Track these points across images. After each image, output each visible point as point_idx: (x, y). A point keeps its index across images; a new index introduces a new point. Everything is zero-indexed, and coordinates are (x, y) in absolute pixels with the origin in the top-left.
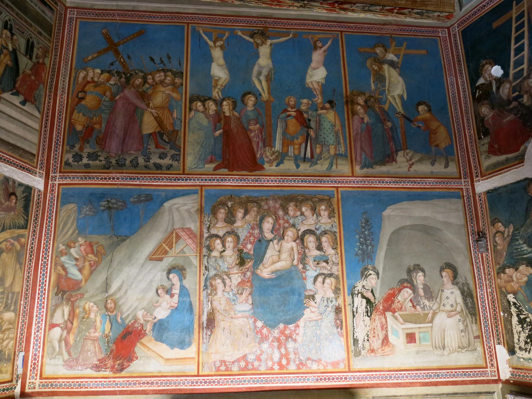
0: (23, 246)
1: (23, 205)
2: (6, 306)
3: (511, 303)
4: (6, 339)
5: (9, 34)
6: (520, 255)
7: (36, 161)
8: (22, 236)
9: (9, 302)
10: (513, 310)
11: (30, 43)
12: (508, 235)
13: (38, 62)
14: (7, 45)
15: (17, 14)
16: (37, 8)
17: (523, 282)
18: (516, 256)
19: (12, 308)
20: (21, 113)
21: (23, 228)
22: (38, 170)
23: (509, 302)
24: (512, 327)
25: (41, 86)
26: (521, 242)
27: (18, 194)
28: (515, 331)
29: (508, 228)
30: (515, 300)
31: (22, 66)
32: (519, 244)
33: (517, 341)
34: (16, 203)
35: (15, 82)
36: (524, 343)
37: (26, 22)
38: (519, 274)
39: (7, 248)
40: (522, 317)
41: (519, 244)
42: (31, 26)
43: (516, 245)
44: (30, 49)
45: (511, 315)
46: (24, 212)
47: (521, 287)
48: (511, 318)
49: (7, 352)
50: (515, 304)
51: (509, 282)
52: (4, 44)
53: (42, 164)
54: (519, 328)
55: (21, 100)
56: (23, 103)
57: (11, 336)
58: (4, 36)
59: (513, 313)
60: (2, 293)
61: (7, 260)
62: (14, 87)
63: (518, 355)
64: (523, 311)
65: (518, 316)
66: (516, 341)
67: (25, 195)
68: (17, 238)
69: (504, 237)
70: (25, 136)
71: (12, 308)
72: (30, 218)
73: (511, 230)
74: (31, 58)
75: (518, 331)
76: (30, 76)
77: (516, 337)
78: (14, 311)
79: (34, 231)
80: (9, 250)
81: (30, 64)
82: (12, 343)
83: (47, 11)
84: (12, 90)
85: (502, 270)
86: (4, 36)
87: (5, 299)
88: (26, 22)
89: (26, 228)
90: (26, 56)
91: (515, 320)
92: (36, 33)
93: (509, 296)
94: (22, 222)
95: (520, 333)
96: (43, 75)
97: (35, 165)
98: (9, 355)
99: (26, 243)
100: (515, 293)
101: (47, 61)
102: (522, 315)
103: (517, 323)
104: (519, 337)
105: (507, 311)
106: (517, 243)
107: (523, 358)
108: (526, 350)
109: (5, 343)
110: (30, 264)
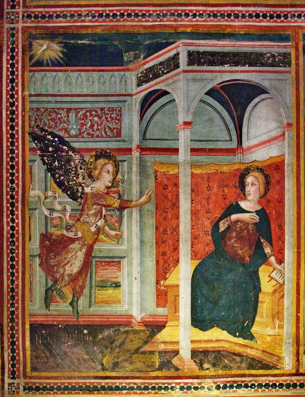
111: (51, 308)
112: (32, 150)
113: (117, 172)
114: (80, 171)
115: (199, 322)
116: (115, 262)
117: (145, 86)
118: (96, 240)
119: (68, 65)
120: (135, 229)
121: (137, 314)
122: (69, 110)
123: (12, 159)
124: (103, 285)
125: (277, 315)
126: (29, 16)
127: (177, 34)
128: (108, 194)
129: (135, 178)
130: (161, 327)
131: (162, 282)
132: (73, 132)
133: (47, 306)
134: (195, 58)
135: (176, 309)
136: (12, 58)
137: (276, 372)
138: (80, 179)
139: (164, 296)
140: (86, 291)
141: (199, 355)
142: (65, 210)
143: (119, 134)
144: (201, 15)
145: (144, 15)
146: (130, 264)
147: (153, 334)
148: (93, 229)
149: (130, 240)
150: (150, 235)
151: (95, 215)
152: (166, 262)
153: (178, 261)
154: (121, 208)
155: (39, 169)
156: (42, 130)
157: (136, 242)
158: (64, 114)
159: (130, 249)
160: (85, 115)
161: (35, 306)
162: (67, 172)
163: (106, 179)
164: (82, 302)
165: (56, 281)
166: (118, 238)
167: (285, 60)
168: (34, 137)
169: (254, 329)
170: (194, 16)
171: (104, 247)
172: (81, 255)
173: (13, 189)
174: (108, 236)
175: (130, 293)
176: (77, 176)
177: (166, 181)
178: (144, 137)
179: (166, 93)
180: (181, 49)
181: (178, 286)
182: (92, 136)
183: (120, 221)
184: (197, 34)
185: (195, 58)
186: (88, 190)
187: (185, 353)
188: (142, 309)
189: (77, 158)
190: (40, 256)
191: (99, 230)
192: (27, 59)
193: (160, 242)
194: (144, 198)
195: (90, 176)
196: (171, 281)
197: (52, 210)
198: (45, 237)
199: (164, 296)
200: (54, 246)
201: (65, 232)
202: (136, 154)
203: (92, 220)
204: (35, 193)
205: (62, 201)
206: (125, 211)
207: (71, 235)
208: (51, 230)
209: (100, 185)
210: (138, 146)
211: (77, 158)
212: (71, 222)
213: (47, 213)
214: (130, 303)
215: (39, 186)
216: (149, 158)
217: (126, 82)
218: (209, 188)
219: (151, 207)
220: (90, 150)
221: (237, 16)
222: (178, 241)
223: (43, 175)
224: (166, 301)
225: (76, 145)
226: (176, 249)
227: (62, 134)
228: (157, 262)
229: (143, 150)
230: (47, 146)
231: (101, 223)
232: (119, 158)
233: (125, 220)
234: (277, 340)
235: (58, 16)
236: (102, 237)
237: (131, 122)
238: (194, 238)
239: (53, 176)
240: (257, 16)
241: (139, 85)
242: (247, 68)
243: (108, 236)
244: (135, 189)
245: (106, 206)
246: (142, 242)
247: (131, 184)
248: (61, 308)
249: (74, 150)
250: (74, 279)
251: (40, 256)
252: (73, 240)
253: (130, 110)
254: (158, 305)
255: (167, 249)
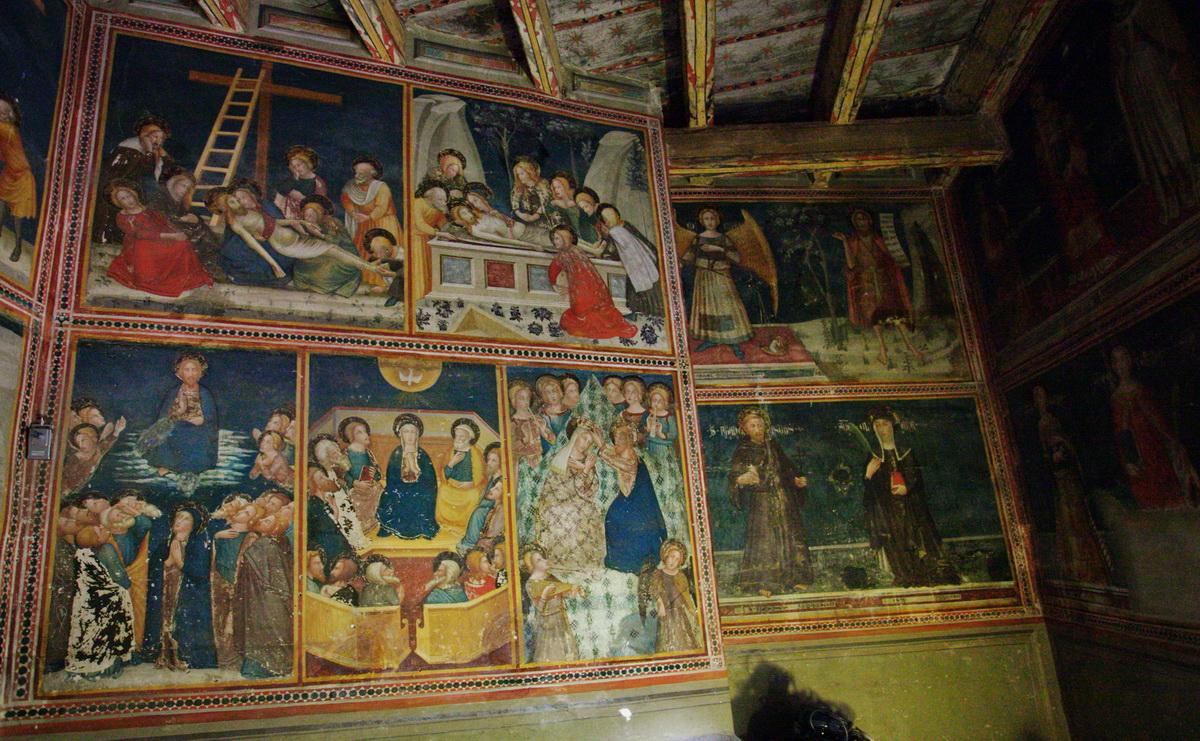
3: (83, 566)
6: (129, 478)
10: (84, 580)
12: (111, 436)
17: (122, 528)
18: (120, 477)
23: (77, 564)
24: (70, 612)
26: (138, 455)
28: (75, 622)
29: (115, 423)
30: (93, 561)
32: (131, 458)
33: (77, 640)
36: (91, 642)
38: (116, 512)
40: (101, 593)
41: (131, 458)
43: (125, 458)
45: (75, 589)
47: (115, 536)
48: (74, 594)
50: (90, 568)
51: (86, 524)
54: (89, 615)
59: (81, 585)
63: (71, 670)
64: (108, 583)
65: (91, 591)
66: (73, 640)
69: (98, 437)
73: (121, 426)
75: (85, 620)
77: (76, 632)
85: (79, 500)
91: (82, 598)
93: (79, 553)
95: (87, 625)
100: (97, 548)
102: (103, 589)
103: (87, 605)
104: (83, 633)
105: (68, 582)
106: (128, 454)
107: (83, 675)
108: (93, 658)
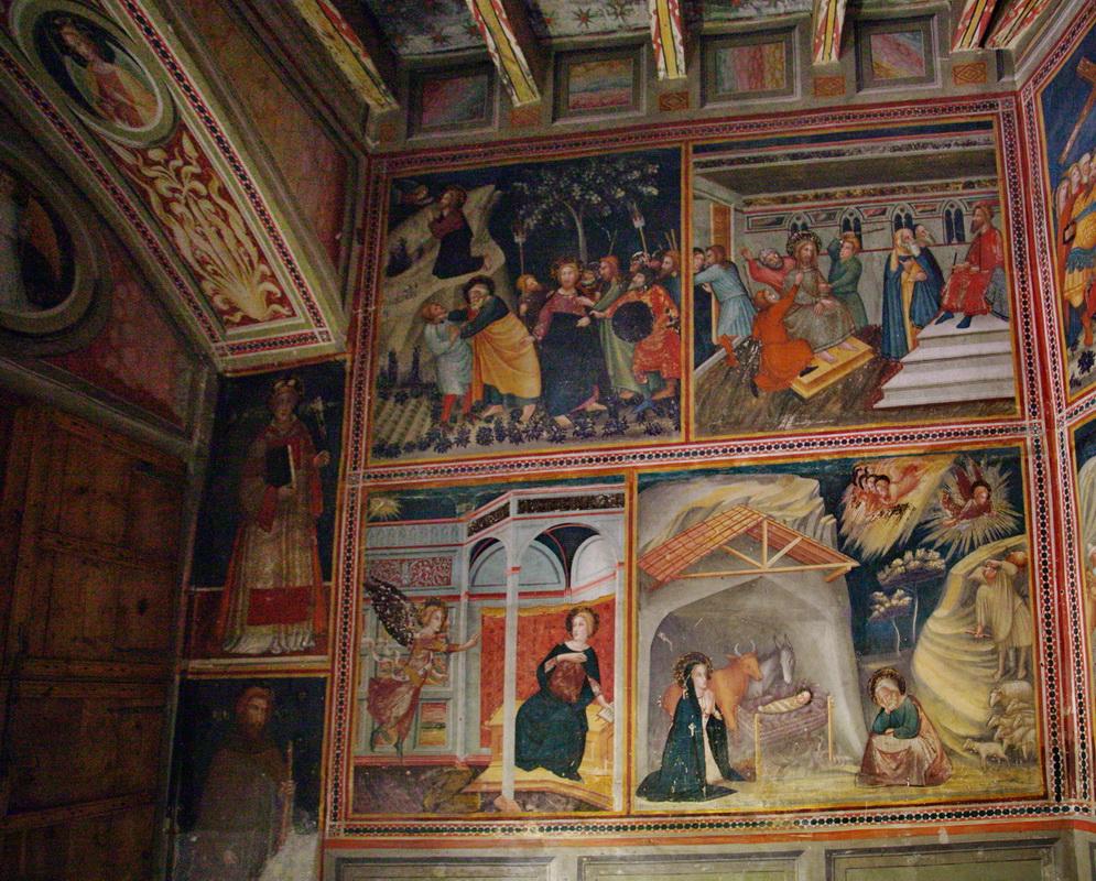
0: (1022, 566)
1: (1004, 495)
2: (1006, 672)
4: (1019, 727)
5: (906, 232)
7: (1018, 407)
8: (1016, 548)
9: (1012, 664)
11: (953, 217)
13: (980, 235)
14: (908, 251)
15: (915, 190)
16: (954, 149)
19: (1021, 673)
20: (964, 343)
21: (1014, 534)
22: (1027, 422)
25: (998, 271)
27: (989, 481)
31: (946, 266)
34: (988, 497)
35: (939, 300)
37: (933, 187)
39: (987, 577)
42: (947, 185)
44: (954, 226)
46: (1010, 505)
49: (1024, 748)
52: (903, 254)
53: (1034, 406)
55: (958, 322)
56: (965, 324)
57: (1031, 721)
58: (899, 242)
60: (994, 652)
61: (991, 596)
62: (939, 305)
67: (1005, 476)
68: (1006, 555)
70: (982, 377)
71: (1021, 673)
72: (1026, 513)
74: (961, 239)
76: (968, 269)
78: (1027, 678)
79: (1043, 532)
80: (990, 580)
81: (963, 250)
82: (1032, 734)
83: (974, 136)
84: (935, 317)
86: (899, 242)
87: (1001, 661)
88: (933, 187)
89: (1021, 531)
90: (949, 243)
92: (960, 191)
94: (1011, 524)
96: (996, 250)
97: (1019, 415)
98: (1030, 754)
99: (1029, 557)
101: (999, 222)
109: (1018, 733)
110: (1047, 593)
111: (376, 750)
112: (365, 599)
113: (446, 618)
114: (411, 619)
115: (523, 762)
116: (440, 703)
117: (476, 535)
118: (424, 683)
119: (403, 519)
120: (461, 671)
121: (461, 755)
122: (402, 561)
123: (347, 608)
124: (428, 726)
125: (606, 754)
126: (369, 477)
127: (510, 485)
128: (436, 638)
129: (463, 623)
130: (483, 767)
131: (486, 723)
132: (405, 582)
133: (372, 748)
134: (525, 507)
135: (500, 749)
136: (351, 515)
137: (604, 813)
138: (410, 626)
139: (488, 737)
140: (411, 733)
141: (522, 796)
142: (394, 655)
143: (449, 583)
144: (533, 464)
145: (477, 469)
146: (455, 705)
147: (476, 775)
148: (421, 673)
149: (455, 682)
150: (476, 677)
151: (424, 659)
152: (491, 702)
153: (502, 702)
154: (448, 652)
155: (371, 618)
156: (376, 580)
157: (461, 684)
158: (397, 565)
159: (456, 690)
160: (417, 565)
161: (360, 748)
162: (398, 620)
163: (436, 625)
164: (407, 743)
165: (382, 723)
166: (445, 680)
167: (618, 500)
168: (368, 587)
169: (581, 770)
170: (527, 465)
171: (429, 690)
172: (408, 697)
173: (345, 637)
174: (434, 679)
175: (455, 734)
176: (407, 622)
177: (492, 625)
178: (472, 581)
179: (496, 541)
180: (512, 499)
181: (502, 726)
182: (423, 584)
183: (447, 664)
184: (529, 483)
185: (525, 507)
186: (417, 636)
187: (508, 794)
188: (466, 749)
189: (408, 606)
190: (368, 700)
191: (426, 674)
192: (365, 516)
193: (485, 683)
194: (471, 642)
195: (420, 623)
196: (496, 719)
197: (382, 656)
198: (374, 681)
199: (488, 737)
200: (381, 690)
201: (393, 676)
202: (464, 600)
203: (420, 664)
204: (367, 639)
205: (392, 647)
206: (452, 655)
207: (399, 679)
208: (380, 674)
209: (429, 631)
210: (467, 593)
211: (408, 606)
212: (400, 667)
213: (377, 658)
214: (454, 744)
215: (371, 634)
216: (478, 603)
217: (458, 533)
218: (535, 630)
219: (477, 650)
220: (422, 598)
221: (569, 463)
222: (503, 682)
223: (374, 622)
224: (490, 742)
225: (407, 594)
226: (501, 690)
227: (394, 584)
228: (482, 703)
229: (471, 596)
230: (380, 596)
231: (428, 666)
232: (449, 604)
233: (452, 663)
234: (606, 781)
235: (396, 475)
236: (429, 680)
237: (461, 570)
238: (520, 678)
239: (384, 623)
240: (591, 460)
241: (469, 535)
242: (578, 511)
243: (434, 679)
244: (463, 634)
245: (434, 651)
246: (468, 684)
247: (458, 630)
248: (387, 749)
249: (405, 598)
250: (400, 721)
251: (368, 700)
252: (400, 684)
253: (460, 558)
254: (482, 746)
255: (491, 690)
